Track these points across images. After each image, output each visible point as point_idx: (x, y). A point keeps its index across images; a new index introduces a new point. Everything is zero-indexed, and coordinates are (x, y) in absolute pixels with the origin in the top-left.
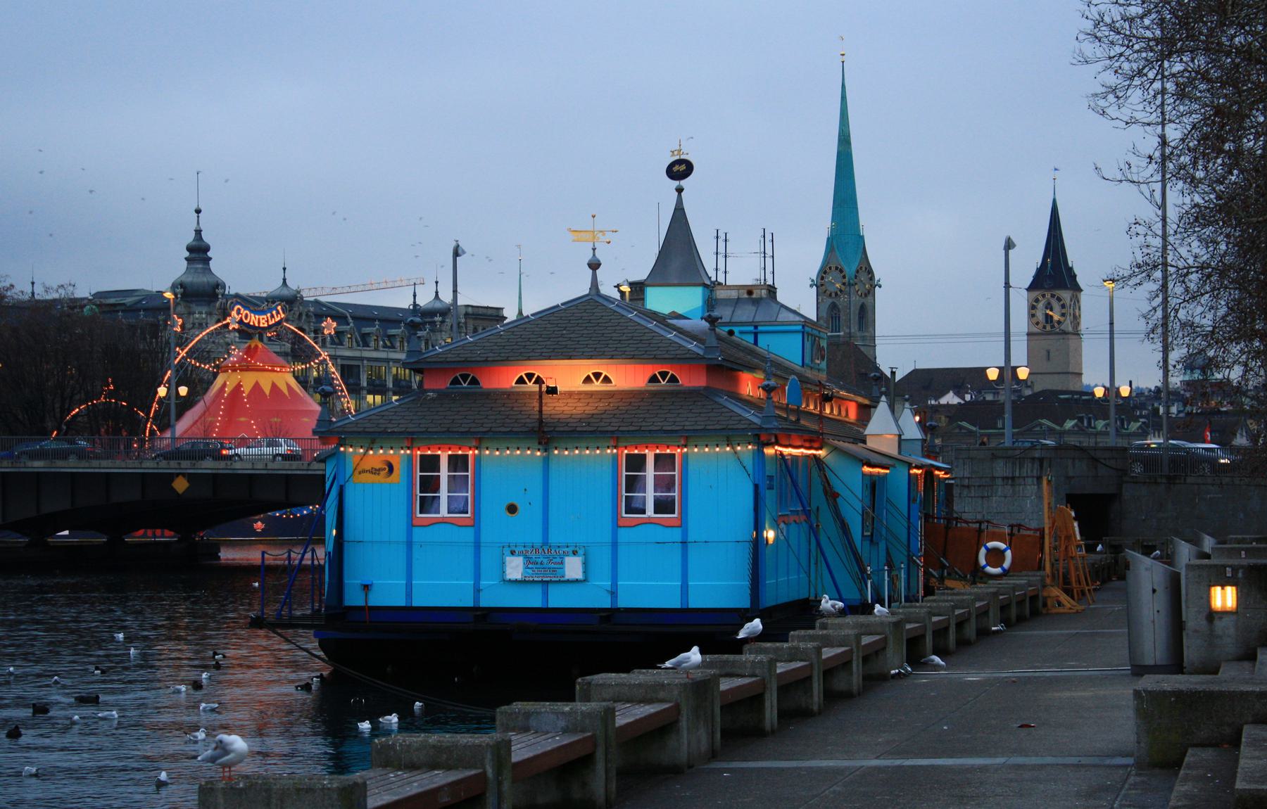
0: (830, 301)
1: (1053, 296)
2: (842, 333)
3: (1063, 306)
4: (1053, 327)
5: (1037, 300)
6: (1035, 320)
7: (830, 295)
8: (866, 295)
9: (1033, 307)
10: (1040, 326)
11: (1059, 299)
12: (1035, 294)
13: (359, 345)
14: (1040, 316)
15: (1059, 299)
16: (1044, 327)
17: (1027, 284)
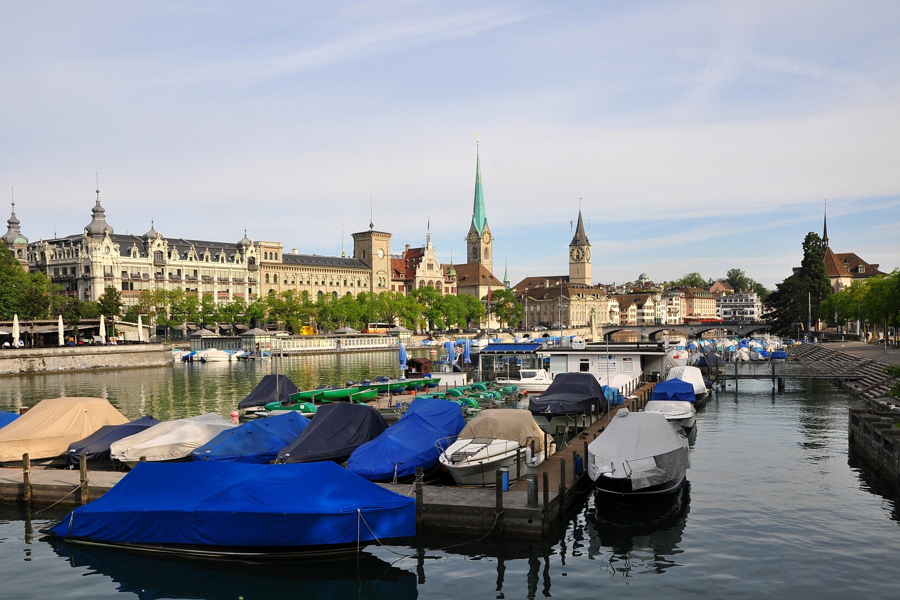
1: (579, 248)
4: (579, 260)
5: (573, 250)
8: (488, 243)
9: (572, 253)
11: (582, 249)
12: (572, 248)
15: (582, 249)
16: (576, 260)
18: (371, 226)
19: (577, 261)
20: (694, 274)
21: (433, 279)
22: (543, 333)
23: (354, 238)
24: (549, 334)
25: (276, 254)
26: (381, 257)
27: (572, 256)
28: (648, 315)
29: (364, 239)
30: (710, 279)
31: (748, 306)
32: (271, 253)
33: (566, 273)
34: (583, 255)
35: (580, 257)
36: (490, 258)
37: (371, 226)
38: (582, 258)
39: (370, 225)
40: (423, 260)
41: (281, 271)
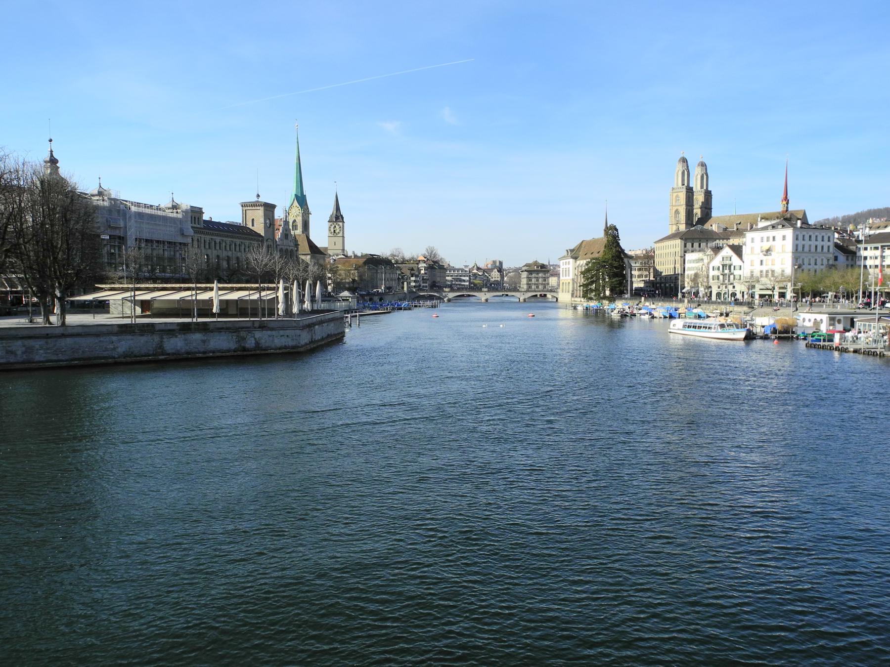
11: (339, 225)
14: (332, 230)
15: (339, 225)
18: (258, 196)
21: (288, 247)
23: (242, 206)
25: (198, 218)
31: (464, 276)
32: (195, 218)
33: (326, 246)
35: (337, 232)
37: (258, 196)
41: (203, 236)
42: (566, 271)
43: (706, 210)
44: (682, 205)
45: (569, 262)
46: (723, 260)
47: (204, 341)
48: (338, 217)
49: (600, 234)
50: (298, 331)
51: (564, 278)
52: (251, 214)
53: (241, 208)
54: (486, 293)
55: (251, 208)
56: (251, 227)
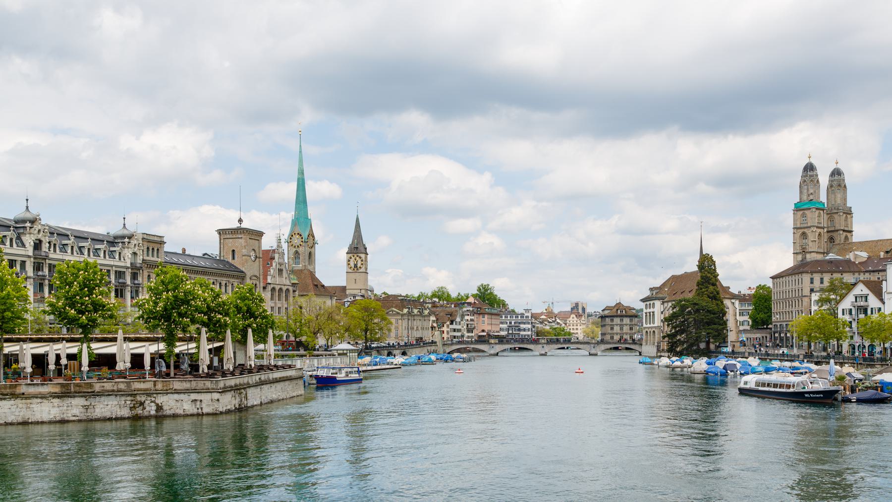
0: (295, 250)
2: (301, 265)
3: (362, 261)
4: (357, 269)
5: (351, 258)
6: (350, 266)
7: (295, 247)
9: (349, 261)
10: (352, 269)
11: (360, 258)
13: (78, 254)
14: (352, 265)
15: (360, 258)
16: (354, 269)
17: (346, 252)
18: (240, 221)
19: (356, 270)
20: (442, 288)
21: (283, 287)
22: (403, 351)
24: (407, 352)
26: (253, 259)
27: (349, 264)
28: (524, 330)
29: (234, 236)
30: (459, 294)
31: (524, 323)
33: (344, 284)
34: (362, 264)
35: (359, 266)
36: (314, 264)
37: (240, 221)
38: (360, 267)
39: (239, 221)
40: (274, 264)
42: (650, 315)
43: (845, 234)
44: (810, 227)
45: (654, 304)
46: (856, 301)
47: (86, 408)
48: (357, 249)
49: (692, 266)
50: (215, 394)
51: (648, 325)
52: (231, 244)
53: (218, 236)
54: (545, 345)
55: (231, 236)
56: (230, 260)
